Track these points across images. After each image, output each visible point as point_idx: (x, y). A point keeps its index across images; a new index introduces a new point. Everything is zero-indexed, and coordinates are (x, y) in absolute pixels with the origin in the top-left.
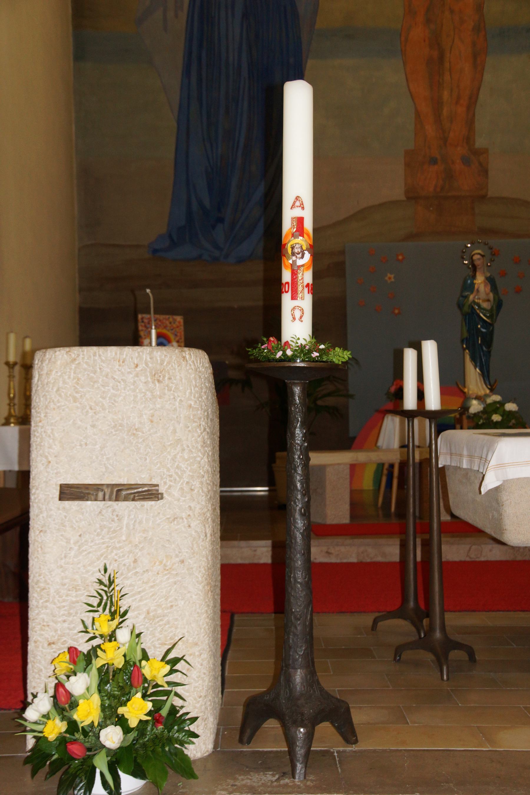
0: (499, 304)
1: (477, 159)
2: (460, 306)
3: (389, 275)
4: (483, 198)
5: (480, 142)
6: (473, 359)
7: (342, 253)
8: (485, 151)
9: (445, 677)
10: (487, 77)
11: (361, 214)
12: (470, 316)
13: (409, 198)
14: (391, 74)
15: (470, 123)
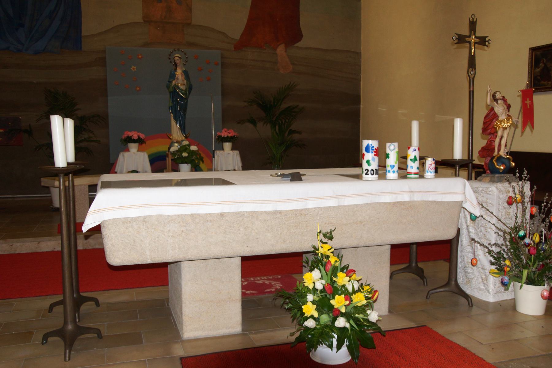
0: (190, 88)
2: (168, 87)
3: (133, 67)
4: (189, 24)
6: (175, 119)
7: (104, 51)
9: (67, 359)
12: (174, 93)
13: (145, 21)
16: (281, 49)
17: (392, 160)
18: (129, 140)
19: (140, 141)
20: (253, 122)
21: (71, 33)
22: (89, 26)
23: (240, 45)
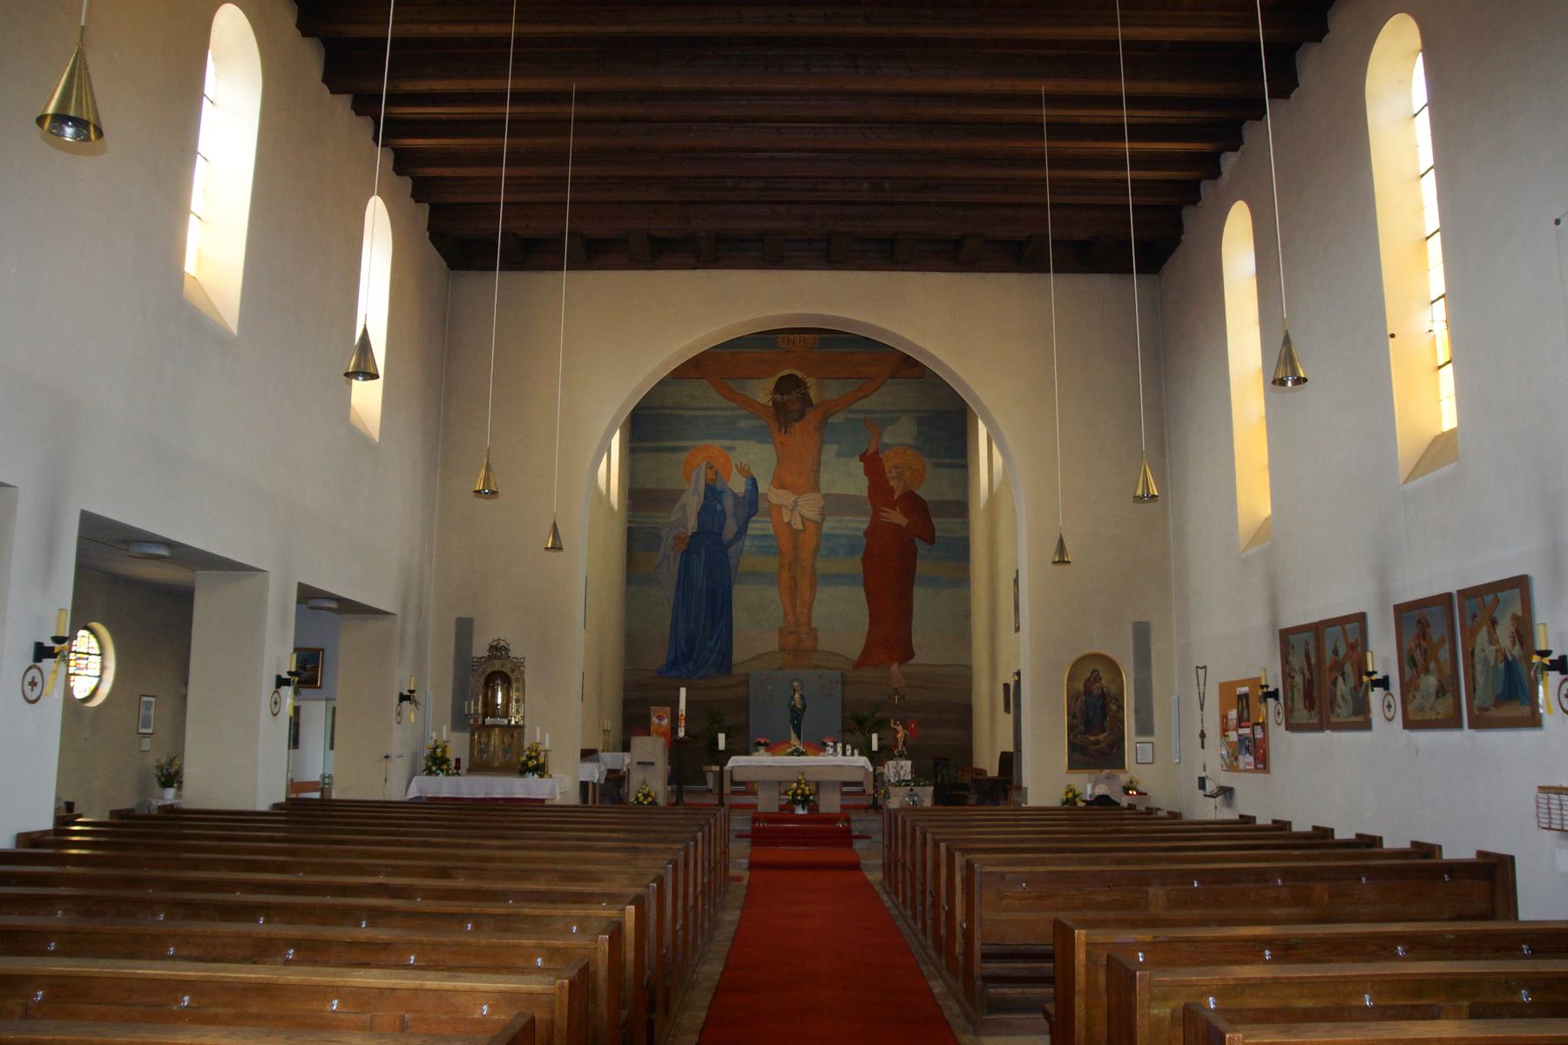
0: (804, 706)
4: (815, 650)
5: (814, 625)
12: (793, 710)
14: (772, 593)
15: (810, 617)
16: (895, 667)
18: (759, 744)
19: (766, 744)
21: (724, 662)
22: (738, 656)
23: (858, 665)
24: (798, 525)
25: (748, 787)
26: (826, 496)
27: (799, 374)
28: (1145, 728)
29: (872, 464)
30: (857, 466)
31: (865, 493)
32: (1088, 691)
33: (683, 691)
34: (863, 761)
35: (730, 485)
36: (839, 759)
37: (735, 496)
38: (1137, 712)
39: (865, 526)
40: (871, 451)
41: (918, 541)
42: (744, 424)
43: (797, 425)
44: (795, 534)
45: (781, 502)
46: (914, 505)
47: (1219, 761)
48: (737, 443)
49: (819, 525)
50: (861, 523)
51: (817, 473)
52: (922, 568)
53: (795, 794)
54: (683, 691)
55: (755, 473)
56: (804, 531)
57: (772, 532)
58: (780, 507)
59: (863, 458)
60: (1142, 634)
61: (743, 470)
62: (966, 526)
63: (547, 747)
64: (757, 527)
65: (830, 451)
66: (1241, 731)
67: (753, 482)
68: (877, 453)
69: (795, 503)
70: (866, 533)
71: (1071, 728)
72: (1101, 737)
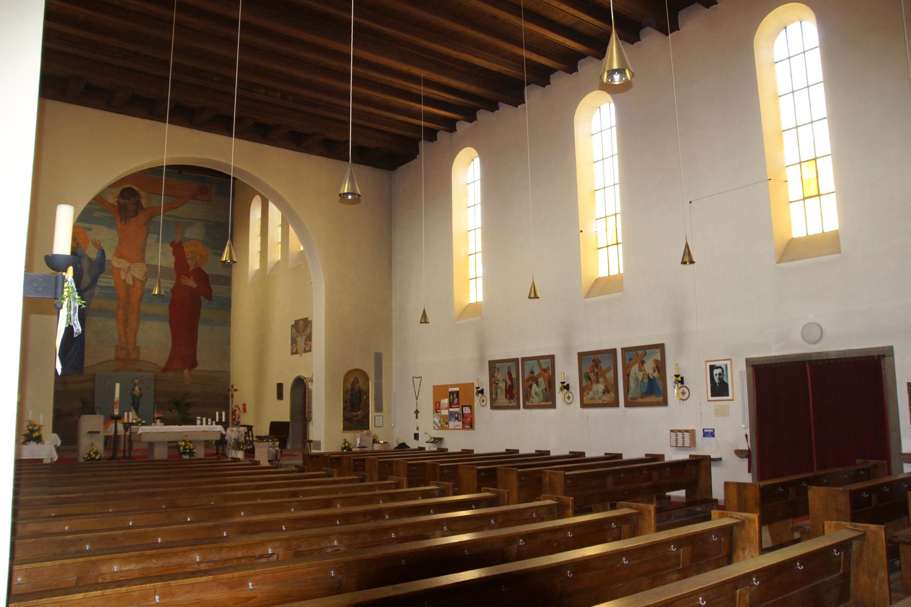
0: (141, 395)
1: (137, 349)
4: (138, 360)
8: (139, 347)
10: (141, 326)
11: (101, 363)
12: (134, 397)
14: (112, 323)
15: (135, 338)
16: (186, 371)
17: (204, 421)
20: (170, 410)
23: (165, 370)
24: (130, 282)
25: (151, 445)
26: (148, 266)
27: (136, 188)
28: (379, 408)
29: (178, 249)
30: (169, 250)
31: (173, 266)
32: (353, 389)
33: (118, 386)
34: (220, 428)
35: (87, 252)
36: (204, 427)
37: (90, 260)
38: (375, 400)
39: (172, 286)
40: (178, 241)
41: (203, 298)
42: (98, 214)
43: (133, 219)
44: (129, 287)
45: (119, 266)
46: (202, 277)
47: (431, 425)
48: (92, 226)
49: (143, 283)
50: (170, 284)
51: (144, 251)
52: (204, 313)
53: (185, 448)
54: (118, 386)
55: (105, 246)
56: (133, 286)
57: (113, 285)
58: (119, 270)
59: (172, 245)
60: (378, 358)
61: (97, 244)
62: (230, 291)
63: (41, 423)
64: (103, 281)
65: (152, 238)
66: (451, 410)
67: (102, 253)
68: (181, 242)
69: (129, 268)
70: (172, 290)
71: (344, 409)
72: (359, 413)
